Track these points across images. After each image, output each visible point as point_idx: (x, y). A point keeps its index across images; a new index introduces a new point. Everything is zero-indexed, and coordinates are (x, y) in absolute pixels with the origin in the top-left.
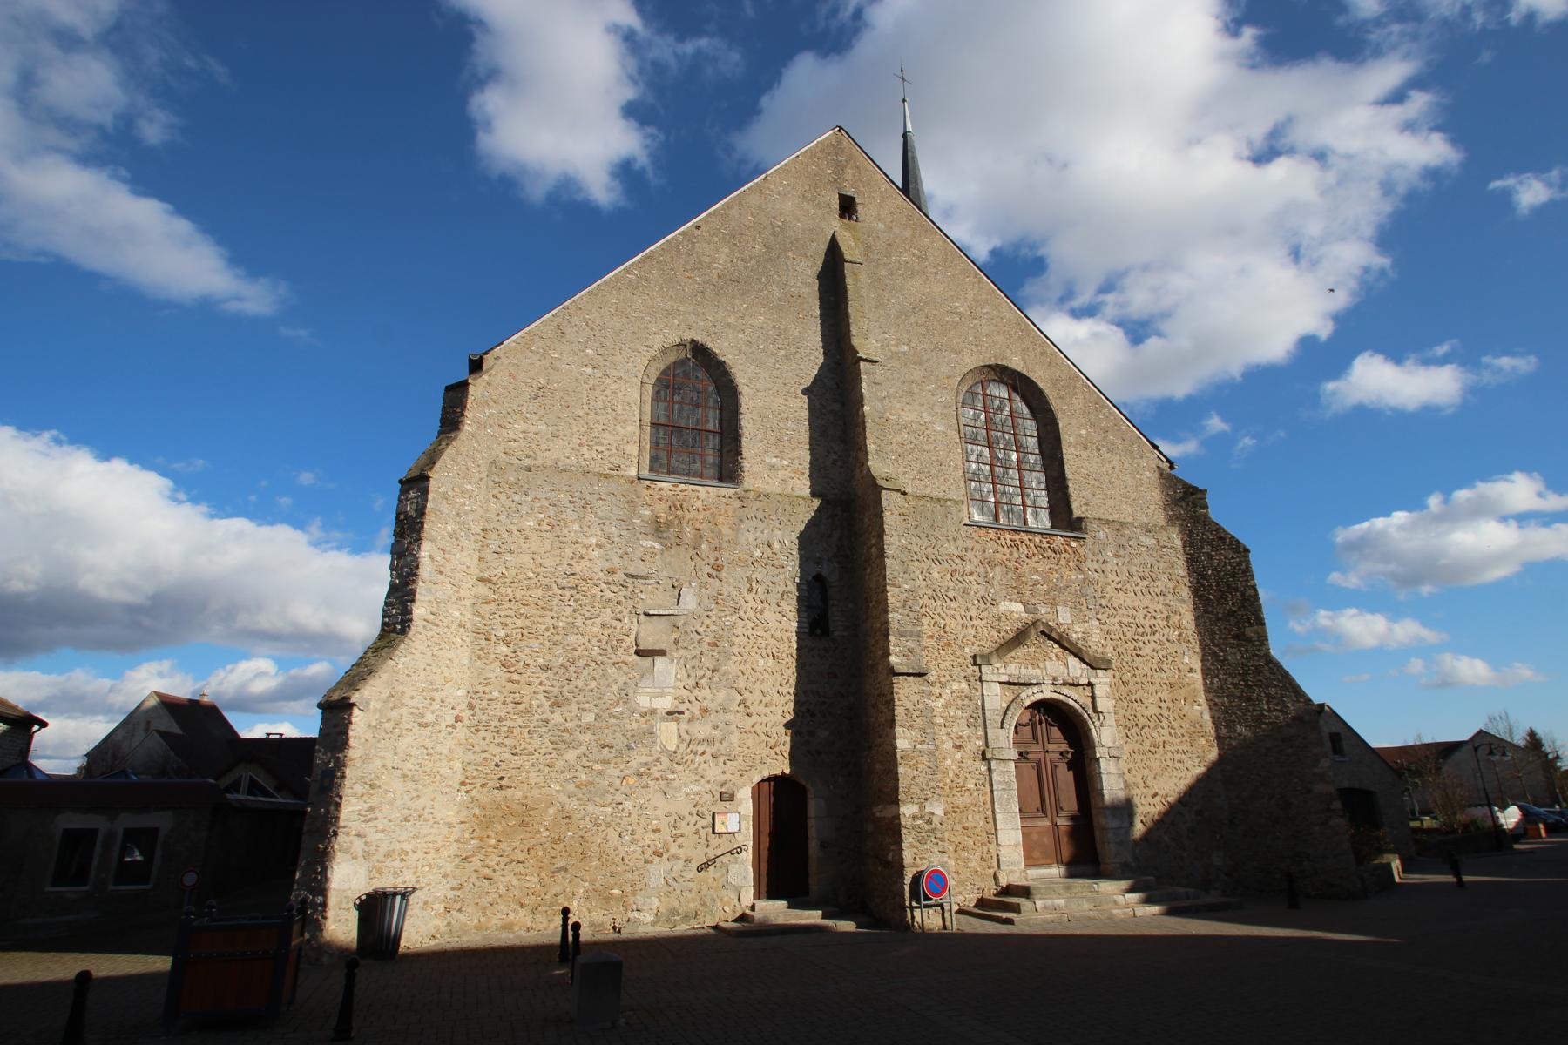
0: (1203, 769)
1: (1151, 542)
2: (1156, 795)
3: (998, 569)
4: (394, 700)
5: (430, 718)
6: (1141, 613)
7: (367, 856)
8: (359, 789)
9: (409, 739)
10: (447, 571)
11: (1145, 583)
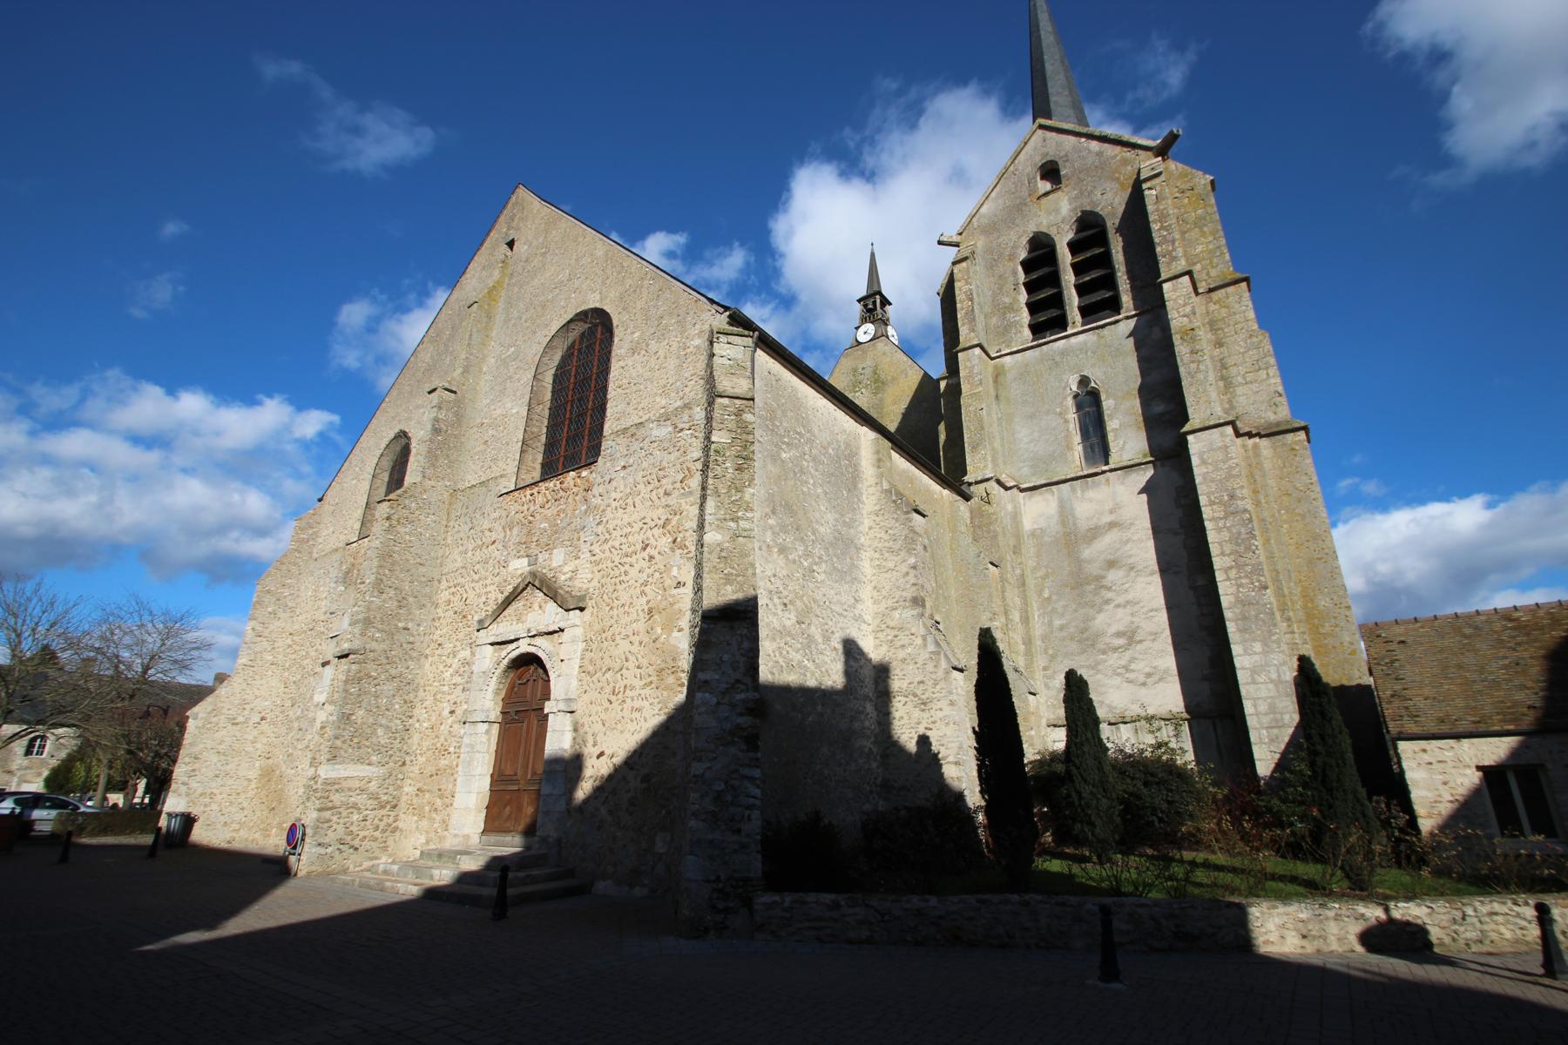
0: (661, 718)
1: (663, 431)
2: (601, 754)
3: (515, 531)
4: (215, 711)
5: (240, 719)
6: (636, 527)
7: (188, 795)
8: (187, 760)
9: (224, 732)
10: (266, 633)
11: (650, 487)
